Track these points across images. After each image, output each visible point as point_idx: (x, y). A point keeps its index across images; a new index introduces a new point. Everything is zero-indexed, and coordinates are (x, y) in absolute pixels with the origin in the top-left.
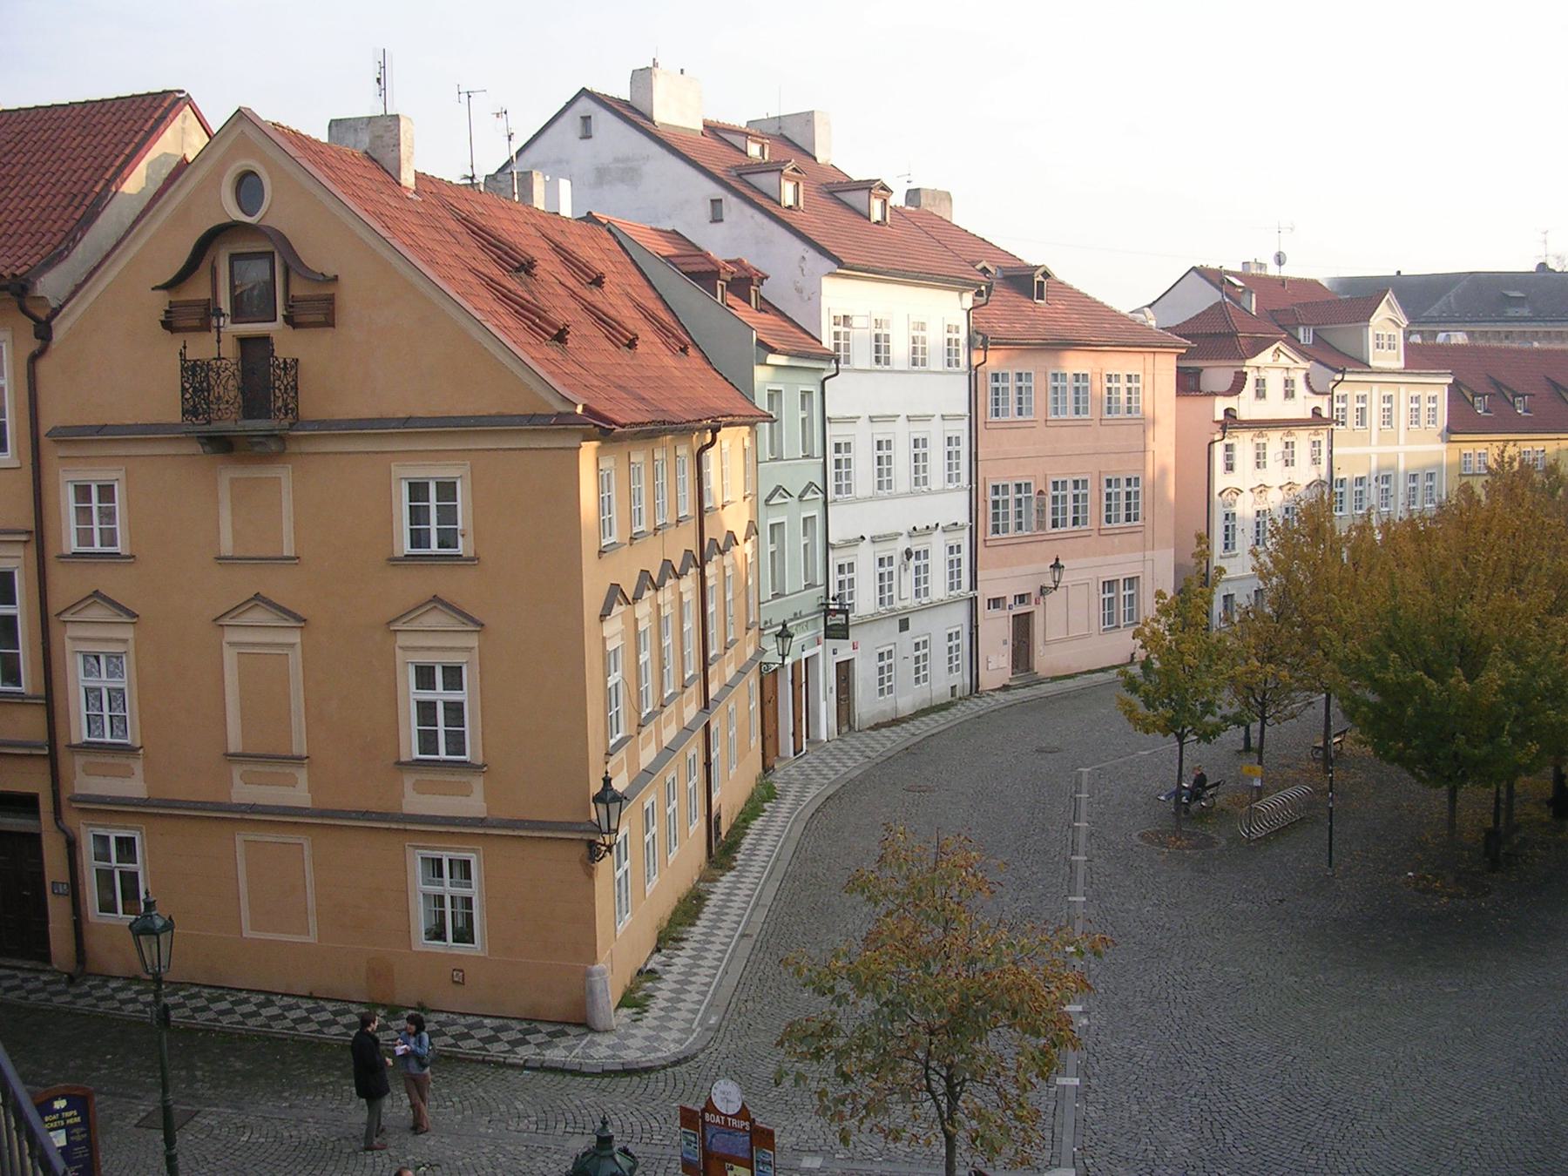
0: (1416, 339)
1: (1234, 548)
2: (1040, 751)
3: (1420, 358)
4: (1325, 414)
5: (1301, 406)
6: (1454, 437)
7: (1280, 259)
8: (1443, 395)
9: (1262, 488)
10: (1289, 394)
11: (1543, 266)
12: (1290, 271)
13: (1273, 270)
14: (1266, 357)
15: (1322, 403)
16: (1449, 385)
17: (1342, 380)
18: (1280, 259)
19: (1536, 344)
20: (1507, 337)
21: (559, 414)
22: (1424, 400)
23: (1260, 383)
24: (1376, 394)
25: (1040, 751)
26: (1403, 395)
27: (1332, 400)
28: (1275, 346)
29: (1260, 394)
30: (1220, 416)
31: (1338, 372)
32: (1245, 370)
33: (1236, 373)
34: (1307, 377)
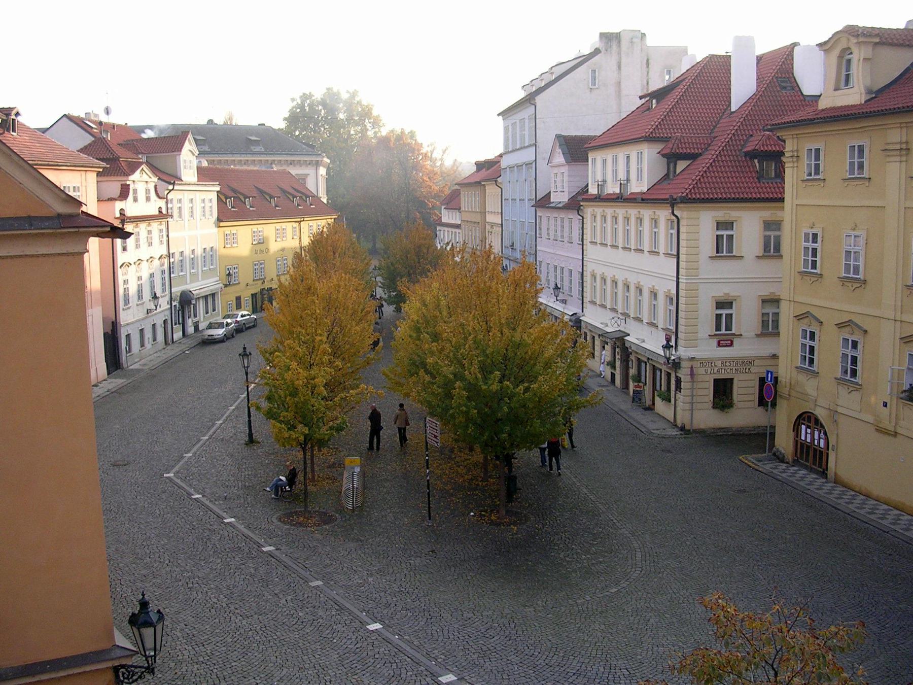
0: (205, 164)
1: (129, 303)
2: (115, 465)
3: (204, 174)
4: (164, 212)
5: (151, 209)
6: (222, 224)
7: (107, 111)
8: (214, 197)
9: (140, 261)
10: (148, 199)
11: (210, 122)
12: (113, 119)
13: (104, 118)
14: (136, 176)
15: (162, 203)
16: (218, 192)
17: (173, 189)
18: (107, 111)
19: (232, 167)
20: (245, 164)
21: (59, 216)
22: (207, 201)
23: (135, 191)
24: (186, 196)
25: (115, 465)
26: (199, 197)
27: (167, 203)
28: (141, 169)
29: (135, 200)
30: (118, 215)
31: (170, 183)
32: (128, 183)
33: (121, 185)
34: (156, 187)
